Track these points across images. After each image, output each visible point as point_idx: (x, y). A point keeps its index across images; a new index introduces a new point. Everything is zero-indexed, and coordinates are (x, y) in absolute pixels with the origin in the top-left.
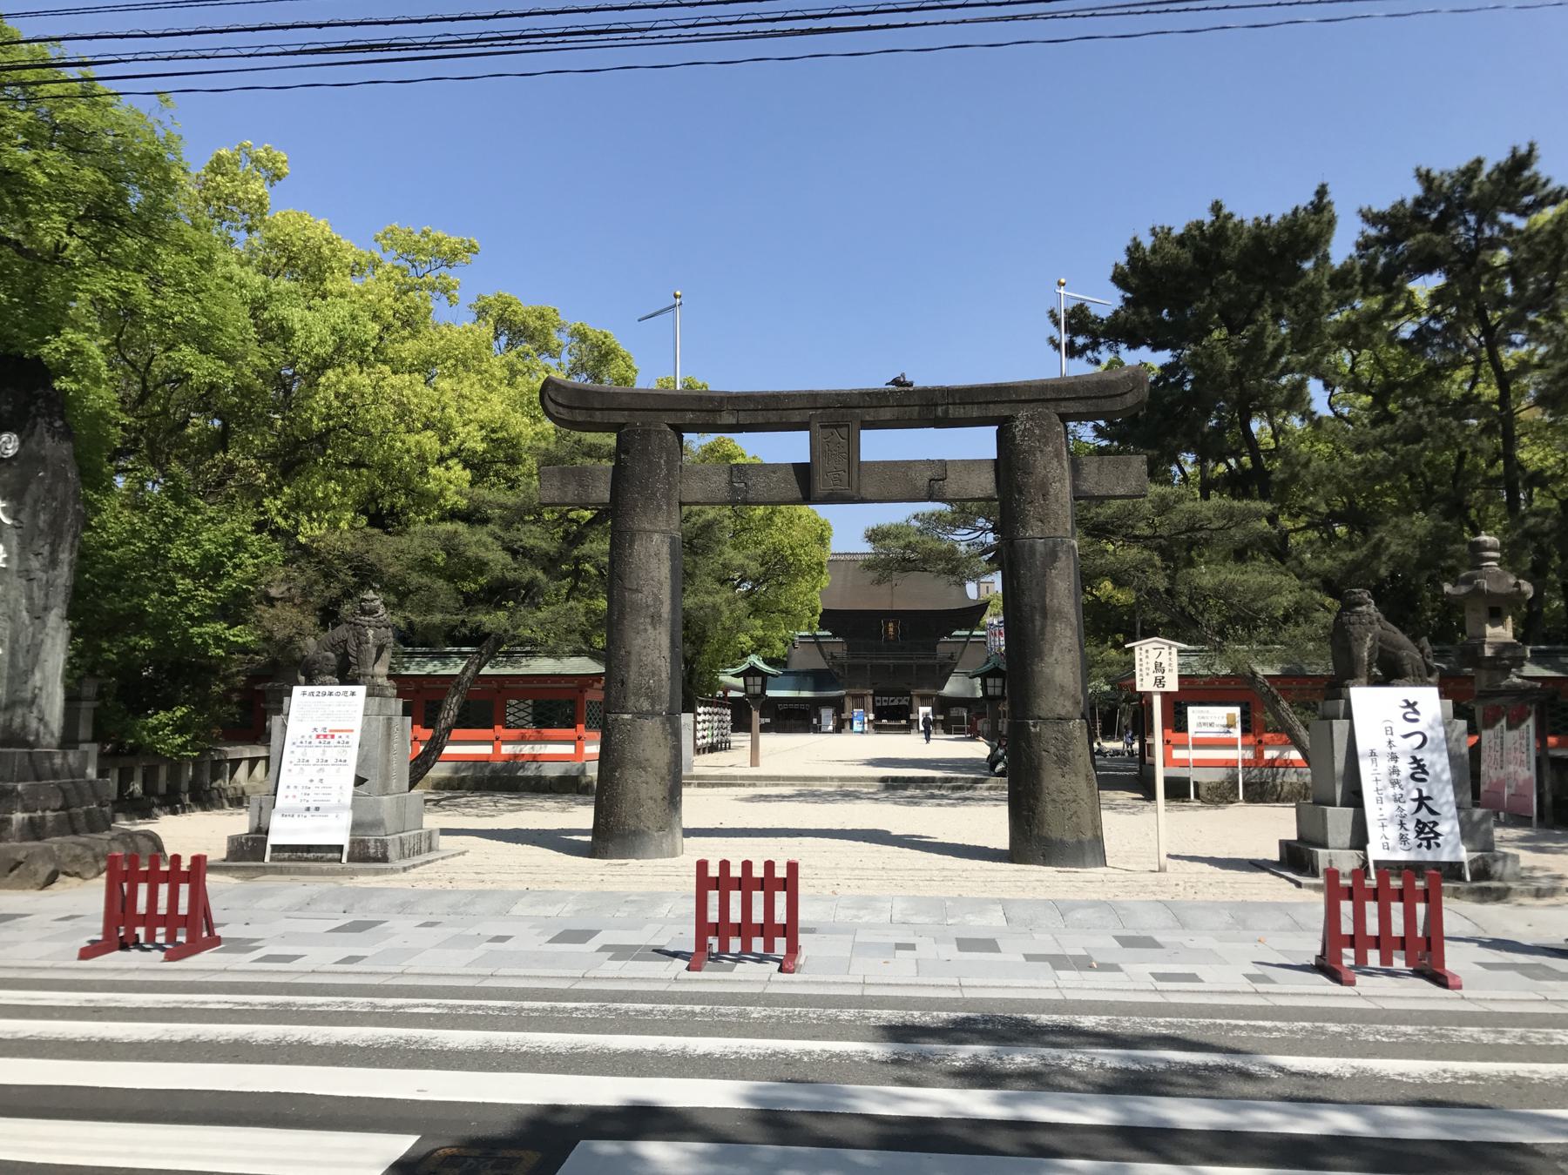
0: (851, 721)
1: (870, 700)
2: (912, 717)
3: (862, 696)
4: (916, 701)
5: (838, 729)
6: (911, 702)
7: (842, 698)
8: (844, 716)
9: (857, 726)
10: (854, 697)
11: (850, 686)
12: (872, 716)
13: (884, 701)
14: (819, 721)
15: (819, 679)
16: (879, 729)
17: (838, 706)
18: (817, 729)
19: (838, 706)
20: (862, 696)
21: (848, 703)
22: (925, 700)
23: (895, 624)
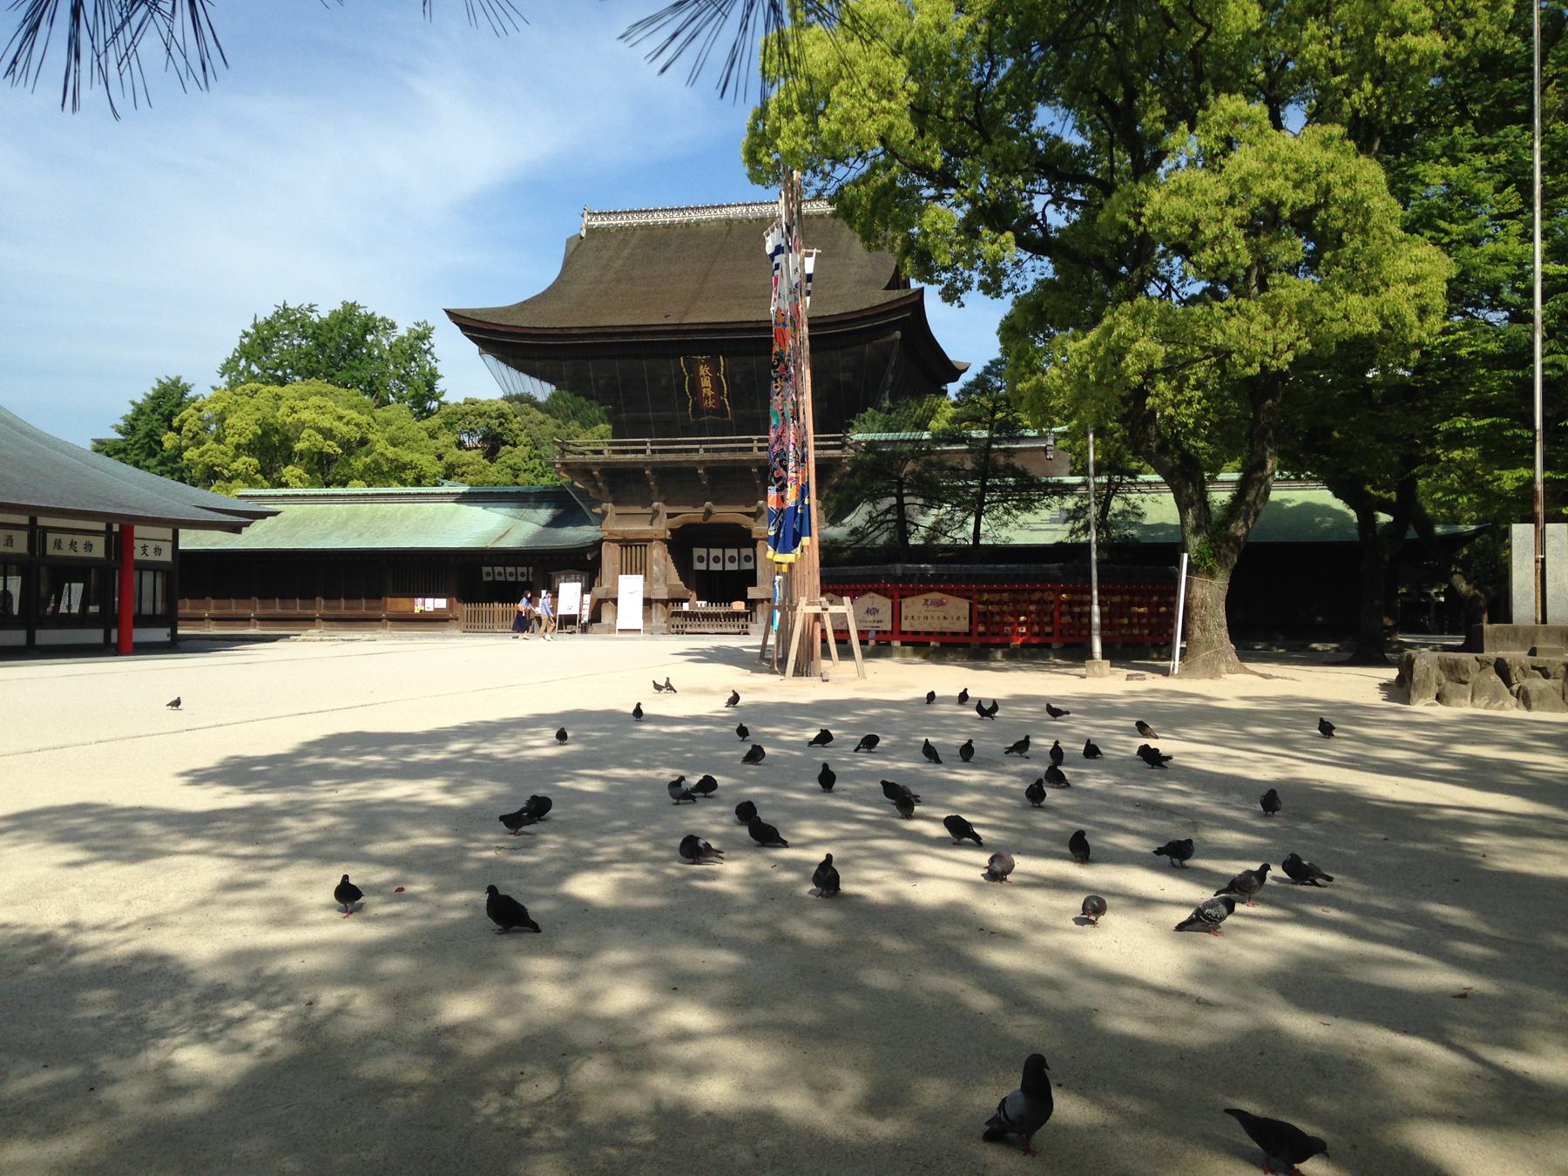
1: (658, 555)
7: (597, 545)
15: (567, 508)
21: (610, 554)
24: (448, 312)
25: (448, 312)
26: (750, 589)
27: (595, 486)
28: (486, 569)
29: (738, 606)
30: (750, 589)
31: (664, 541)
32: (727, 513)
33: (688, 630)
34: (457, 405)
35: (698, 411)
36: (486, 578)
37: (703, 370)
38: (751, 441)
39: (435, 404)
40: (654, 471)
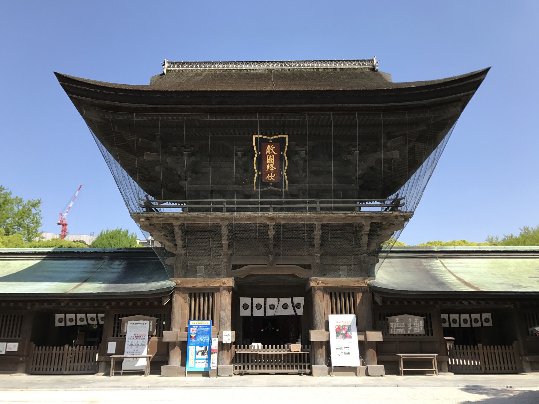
0: (184, 347)
1: (225, 301)
2: (315, 336)
3: (210, 293)
4: (321, 302)
5: (157, 365)
6: (309, 306)
7: (169, 293)
8: (168, 336)
9: (196, 360)
10: (195, 294)
11: (189, 271)
12: (228, 336)
13: (257, 307)
14: (120, 349)
16: (244, 363)
17: (156, 308)
18: (116, 367)
19: (156, 308)
20: (210, 293)
22: (341, 299)
23: (279, 144)
24: (57, 74)
25: (57, 74)
26: (312, 332)
27: (173, 240)
28: (58, 316)
29: (296, 348)
30: (312, 332)
31: (228, 289)
32: (286, 268)
33: (250, 371)
34: (49, 241)
35: (262, 183)
36: (57, 324)
37: (270, 149)
38: (315, 202)
39: (37, 239)
40: (230, 227)
